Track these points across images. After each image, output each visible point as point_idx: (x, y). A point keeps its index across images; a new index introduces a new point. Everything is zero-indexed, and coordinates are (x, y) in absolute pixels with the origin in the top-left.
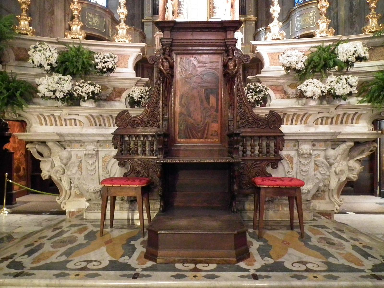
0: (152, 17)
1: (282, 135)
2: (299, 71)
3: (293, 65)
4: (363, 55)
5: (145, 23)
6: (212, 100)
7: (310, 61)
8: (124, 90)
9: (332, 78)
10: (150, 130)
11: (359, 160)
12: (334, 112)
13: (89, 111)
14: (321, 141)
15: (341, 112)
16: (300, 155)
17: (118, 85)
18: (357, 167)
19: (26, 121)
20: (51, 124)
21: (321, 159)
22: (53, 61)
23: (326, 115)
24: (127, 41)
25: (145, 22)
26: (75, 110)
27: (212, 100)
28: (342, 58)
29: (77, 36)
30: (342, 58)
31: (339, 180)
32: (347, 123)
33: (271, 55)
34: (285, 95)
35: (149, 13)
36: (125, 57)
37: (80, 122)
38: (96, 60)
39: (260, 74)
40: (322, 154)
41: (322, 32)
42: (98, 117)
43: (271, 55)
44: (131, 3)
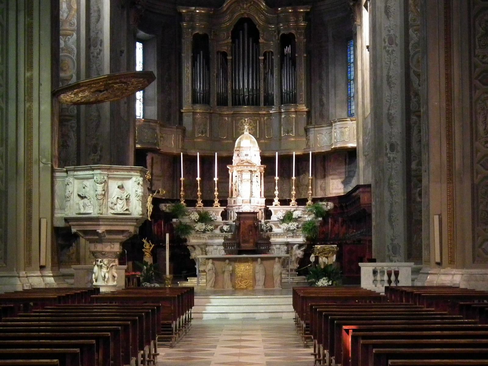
0: (192, 106)
1: (270, 243)
2: (282, 220)
3: (279, 217)
4: (300, 216)
5: (184, 114)
6: (251, 233)
7: (284, 217)
8: (219, 225)
9: (290, 224)
10: (234, 242)
11: (301, 251)
12: (292, 235)
13: (209, 235)
14: (282, 244)
15: (294, 234)
16: (276, 248)
17: (217, 224)
18: (302, 253)
19: (187, 239)
20: (196, 239)
21: (283, 249)
22: (198, 218)
23: (290, 235)
24: (219, 206)
25: (184, 112)
26: (204, 234)
27: (251, 233)
28: (294, 217)
29: (200, 205)
30: (294, 217)
31: (295, 257)
32: (297, 238)
33: (274, 210)
34: (279, 227)
35: (188, 101)
36: (217, 212)
37: (205, 238)
38: (211, 216)
39: (270, 219)
40: (283, 248)
41: (293, 203)
42: (211, 237)
43: (274, 210)
44: (167, 89)
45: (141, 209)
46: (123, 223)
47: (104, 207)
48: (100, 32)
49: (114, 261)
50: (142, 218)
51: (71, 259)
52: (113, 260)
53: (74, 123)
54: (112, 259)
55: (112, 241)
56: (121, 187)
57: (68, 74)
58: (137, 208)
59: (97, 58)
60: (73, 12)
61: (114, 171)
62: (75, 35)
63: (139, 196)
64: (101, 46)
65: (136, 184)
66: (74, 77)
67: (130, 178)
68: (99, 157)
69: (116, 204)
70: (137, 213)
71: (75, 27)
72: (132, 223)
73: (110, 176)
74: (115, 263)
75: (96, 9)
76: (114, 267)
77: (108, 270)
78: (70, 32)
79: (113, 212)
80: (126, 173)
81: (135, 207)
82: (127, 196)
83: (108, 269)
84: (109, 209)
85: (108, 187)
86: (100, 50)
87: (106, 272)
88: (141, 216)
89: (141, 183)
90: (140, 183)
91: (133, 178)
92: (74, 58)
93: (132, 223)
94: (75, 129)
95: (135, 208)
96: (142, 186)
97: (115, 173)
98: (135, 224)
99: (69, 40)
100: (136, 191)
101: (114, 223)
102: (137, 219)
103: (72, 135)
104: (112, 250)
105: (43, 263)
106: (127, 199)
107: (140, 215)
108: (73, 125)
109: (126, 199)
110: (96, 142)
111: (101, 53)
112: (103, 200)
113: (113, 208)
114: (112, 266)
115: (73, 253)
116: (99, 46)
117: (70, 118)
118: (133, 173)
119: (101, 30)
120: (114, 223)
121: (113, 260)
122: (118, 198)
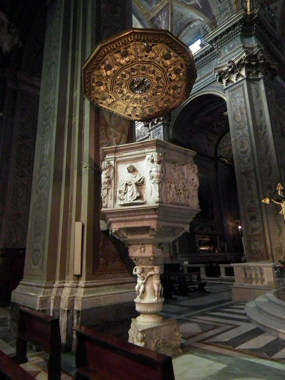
45: (157, 194)
46: (139, 217)
47: (109, 198)
48: (263, 122)
49: (153, 269)
50: (159, 206)
51: (263, 256)
52: (151, 267)
53: (253, 174)
54: (148, 267)
55: (143, 243)
56: (133, 170)
57: (246, 148)
58: (153, 194)
59: (264, 135)
60: (244, 115)
61: (123, 153)
62: (247, 126)
63: (153, 177)
64: (265, 129)
65: (149, 162)
66: (250, 148)
67: (144, 157)
68: (274, 192)
69: (125, 193)
70: (153, 201)
71: (246, 122)
72: (151, 216)
73: (118, 159)
74: (154, 271)
75: (258, 110)
76: (154, 277)
77: (144, 281)
78: (244, 126)
79: (122, 203)
80: (138, 152)
81: (150, 193)
82: (140, 181)
83: (145, 280)
84: (118, 200)
85: (115, 172)
86: (265, 131)
87: (142, 284)
88: (158, 204)
89: (156, 159)
90: (155, 160)
91: (147, 156)
92: (248, 139)
93: (151, 216)
94: (254, 177)
95: (151, 194)
96: (159, 163)
97: (125, 154)
98: (156, 216)
99: (244, 130)
100: (151, 172)
101: (127, 218)
102: (155, 209)
103: (253, 181)
104: (143, 255)
105: (78, 272)
106: (140, 184)
107: (157, 203)
108: (253, 175)
109: (137, 184)
110: (270, 183)
111: (266, 133)
112: (108, 189)
113: (121, 198)
114: (151, 275)
115: (264, 253)
116: (264, 129)
117: (250, 172)
118: (147, 150)
119: (264, 120)
120: (127, 218)
121: (151, 267)
122: (127, 184)
